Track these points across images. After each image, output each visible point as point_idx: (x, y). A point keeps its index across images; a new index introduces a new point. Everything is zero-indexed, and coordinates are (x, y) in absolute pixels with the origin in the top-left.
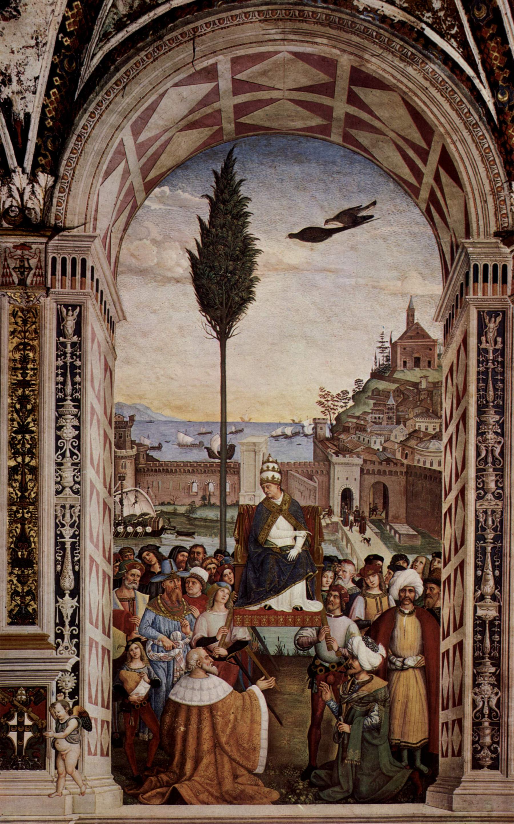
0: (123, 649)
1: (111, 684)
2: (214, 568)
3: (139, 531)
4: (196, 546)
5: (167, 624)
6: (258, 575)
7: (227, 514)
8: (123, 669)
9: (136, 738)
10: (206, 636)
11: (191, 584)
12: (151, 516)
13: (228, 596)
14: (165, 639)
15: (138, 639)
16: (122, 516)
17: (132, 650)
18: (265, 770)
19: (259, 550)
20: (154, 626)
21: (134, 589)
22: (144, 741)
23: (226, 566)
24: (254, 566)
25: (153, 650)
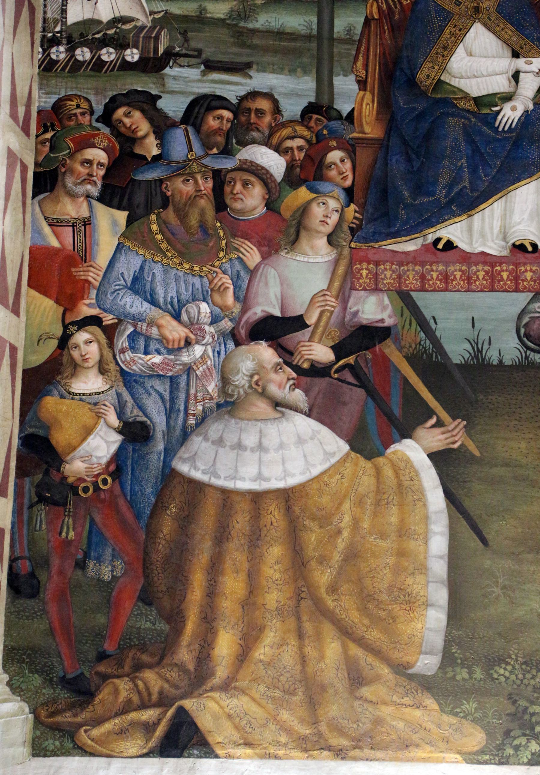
0: (54, 343)
1: (16, 431)
2: (300, 148)
3: (105, 58)
4: (254, 95)
5: (173, 285)
6: (417, 164)
7: (337, 22)
8: (48, 393)
9: (79, 573)
10: (277, 313)
11: (238, 187)
12: (139, 24)
13: (335, 217)
14: (168, 322)
15: (95, 321)
16: (64, 23)
17: (77, 346)
18: (442, 667)
19: (420, 106)
20: (138, 287)
21: (88, 196)
22: (100, 581)
23: (333, 143)
24: (405, 143)
25: (133, 348)
